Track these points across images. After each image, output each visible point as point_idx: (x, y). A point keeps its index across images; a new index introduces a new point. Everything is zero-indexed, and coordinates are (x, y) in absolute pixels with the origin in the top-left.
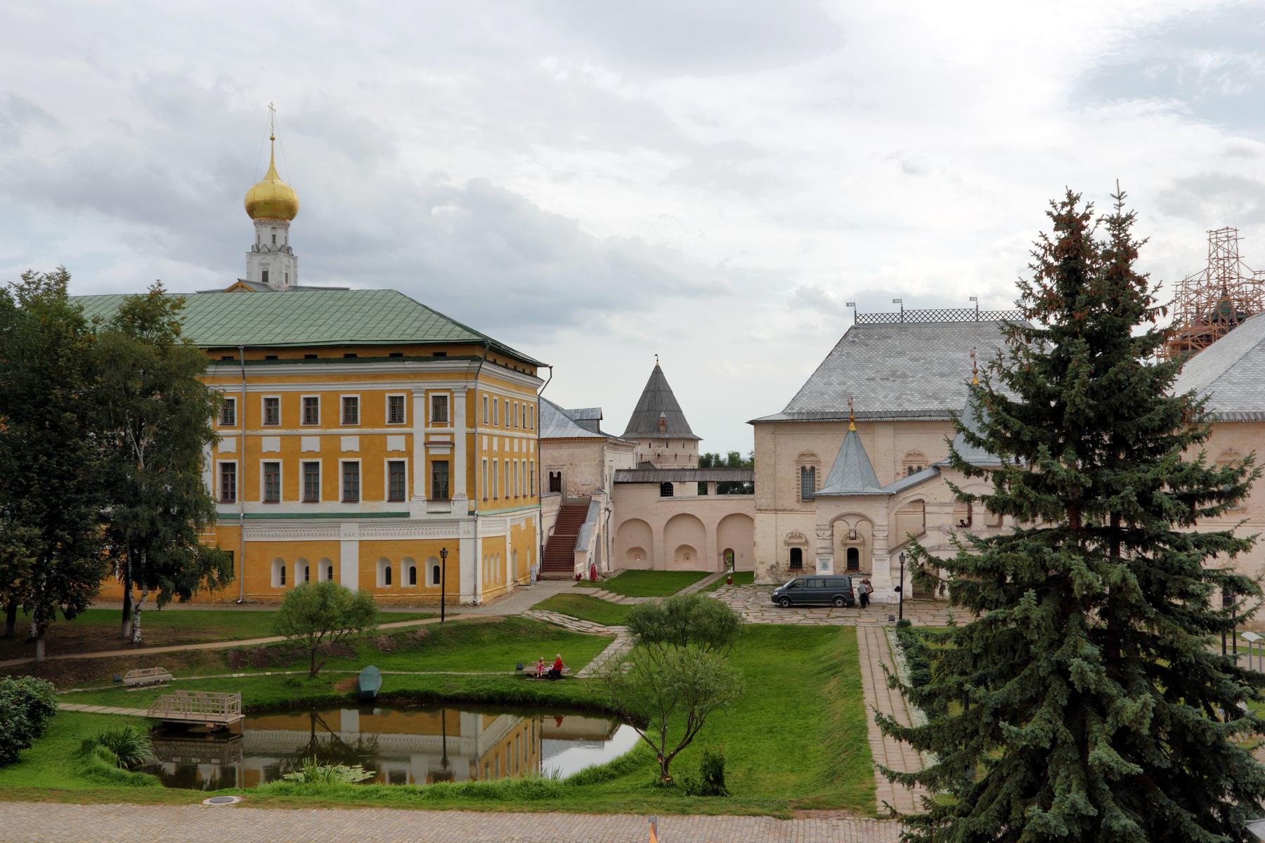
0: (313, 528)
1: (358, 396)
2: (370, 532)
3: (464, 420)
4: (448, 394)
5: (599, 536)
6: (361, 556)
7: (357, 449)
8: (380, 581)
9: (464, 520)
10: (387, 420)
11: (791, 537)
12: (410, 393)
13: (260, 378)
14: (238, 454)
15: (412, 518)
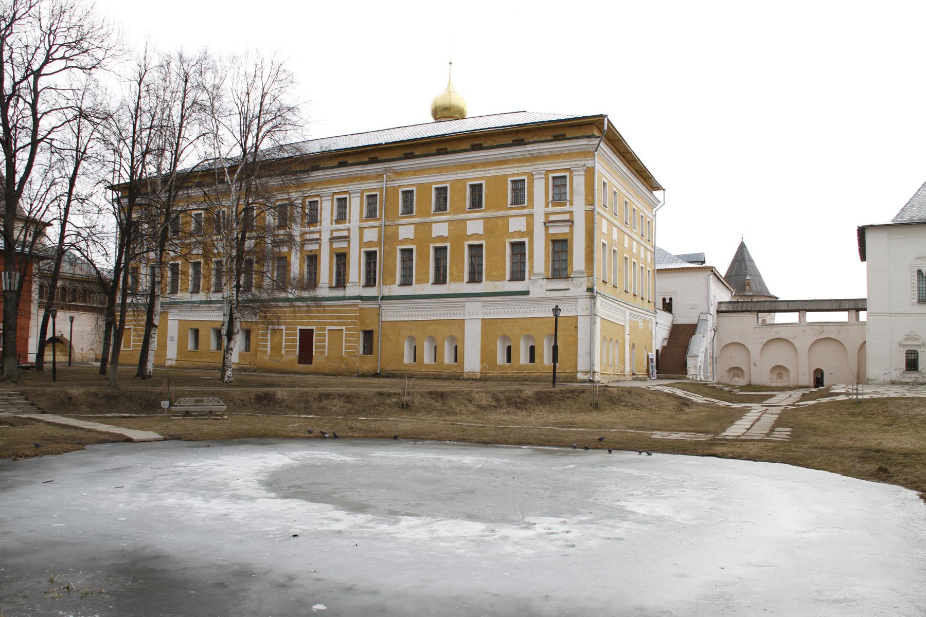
0: (440, 308)
1: (483, 182)
2: (492, 311)
3: (583, 197)
4: (567, 174)
5: (706, 350)
6: (484, 335)
7: (481, 232)
8: (501, 359)
9: (581, 297)
10: (509, 202)
11: (907, 339)
12: (531, 175)
13: (400, 174)
14: (378, 243)
15: (531, 296)
